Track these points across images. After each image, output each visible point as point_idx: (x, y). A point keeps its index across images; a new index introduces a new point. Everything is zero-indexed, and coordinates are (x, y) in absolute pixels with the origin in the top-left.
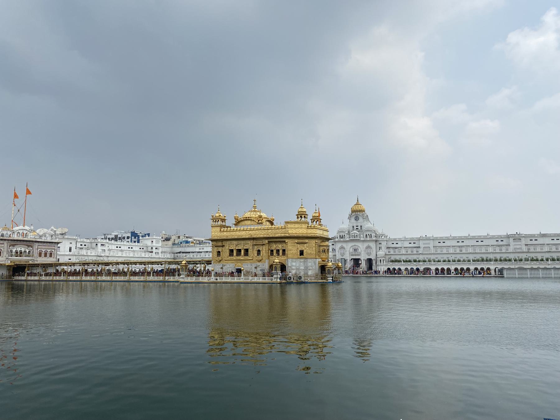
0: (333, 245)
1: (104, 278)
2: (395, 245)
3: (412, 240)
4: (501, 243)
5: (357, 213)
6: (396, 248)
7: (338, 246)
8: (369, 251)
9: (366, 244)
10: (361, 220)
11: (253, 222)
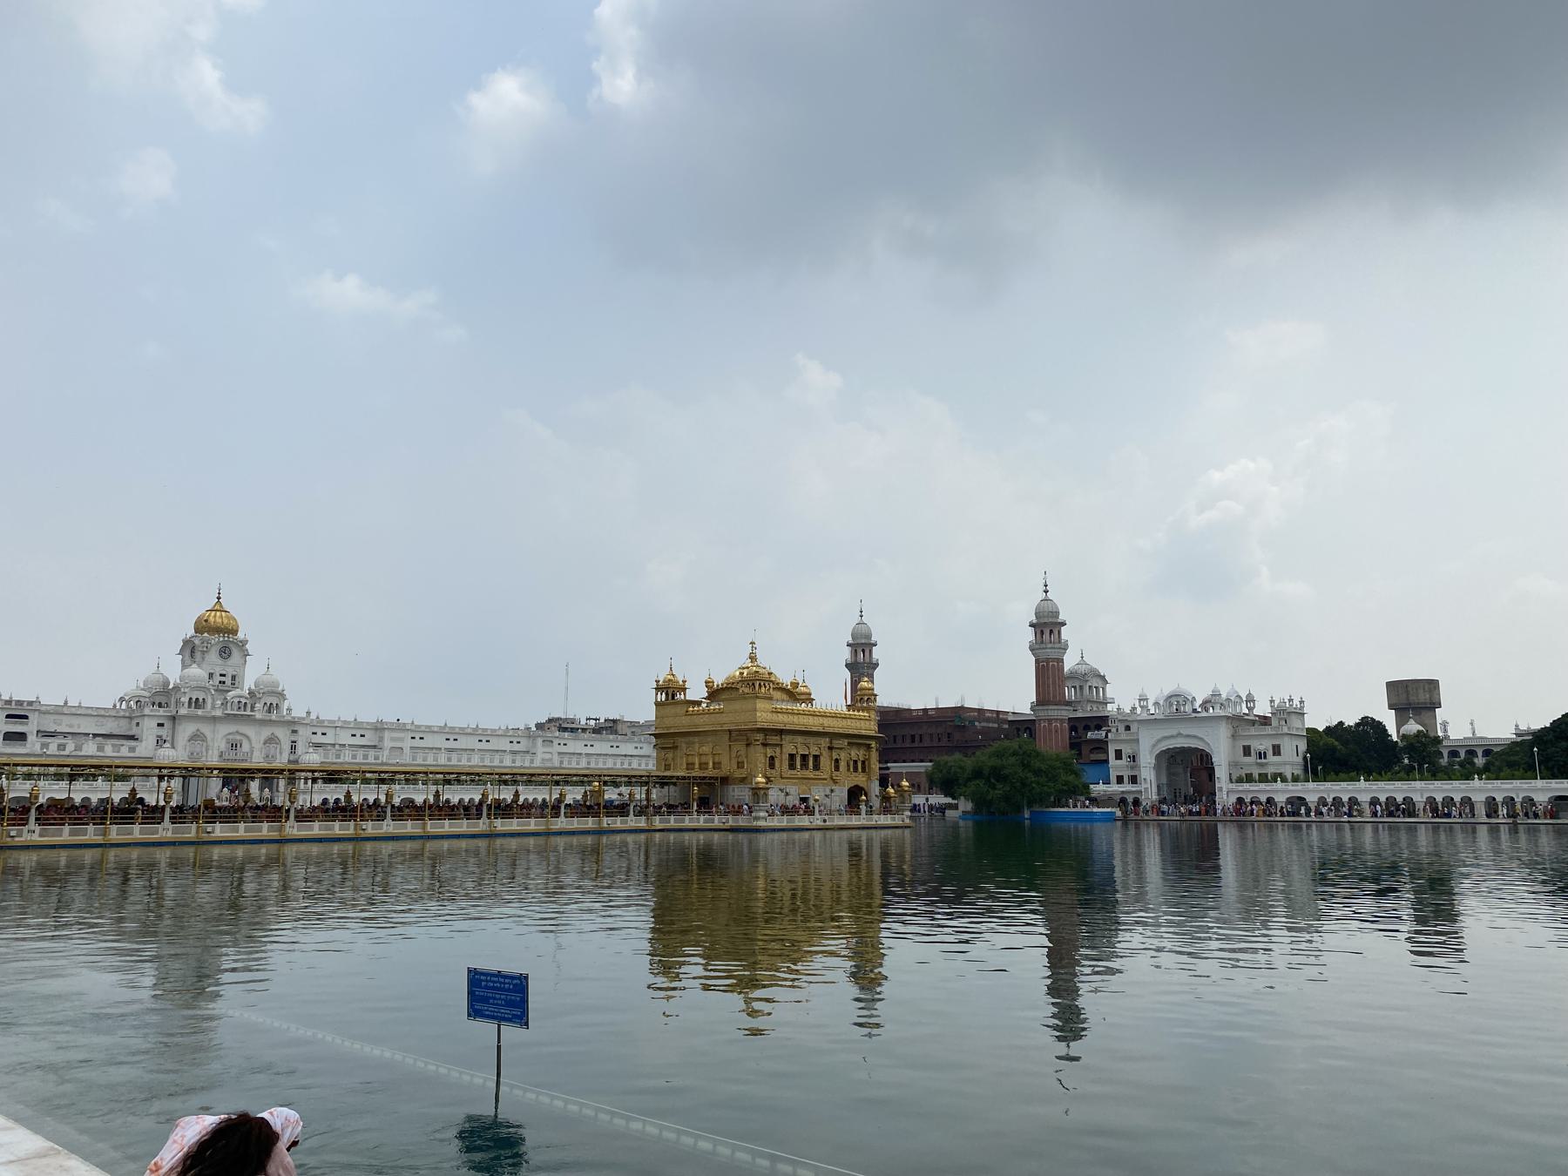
0: (161, 725)
1: (389, 826)
2: (319, 739)
3: (357, 727)
4: (516, 747)
5: (215, 636)
7: (186, 730)
8: (272, 748)
9: (266, 732)
11: (785, 697)
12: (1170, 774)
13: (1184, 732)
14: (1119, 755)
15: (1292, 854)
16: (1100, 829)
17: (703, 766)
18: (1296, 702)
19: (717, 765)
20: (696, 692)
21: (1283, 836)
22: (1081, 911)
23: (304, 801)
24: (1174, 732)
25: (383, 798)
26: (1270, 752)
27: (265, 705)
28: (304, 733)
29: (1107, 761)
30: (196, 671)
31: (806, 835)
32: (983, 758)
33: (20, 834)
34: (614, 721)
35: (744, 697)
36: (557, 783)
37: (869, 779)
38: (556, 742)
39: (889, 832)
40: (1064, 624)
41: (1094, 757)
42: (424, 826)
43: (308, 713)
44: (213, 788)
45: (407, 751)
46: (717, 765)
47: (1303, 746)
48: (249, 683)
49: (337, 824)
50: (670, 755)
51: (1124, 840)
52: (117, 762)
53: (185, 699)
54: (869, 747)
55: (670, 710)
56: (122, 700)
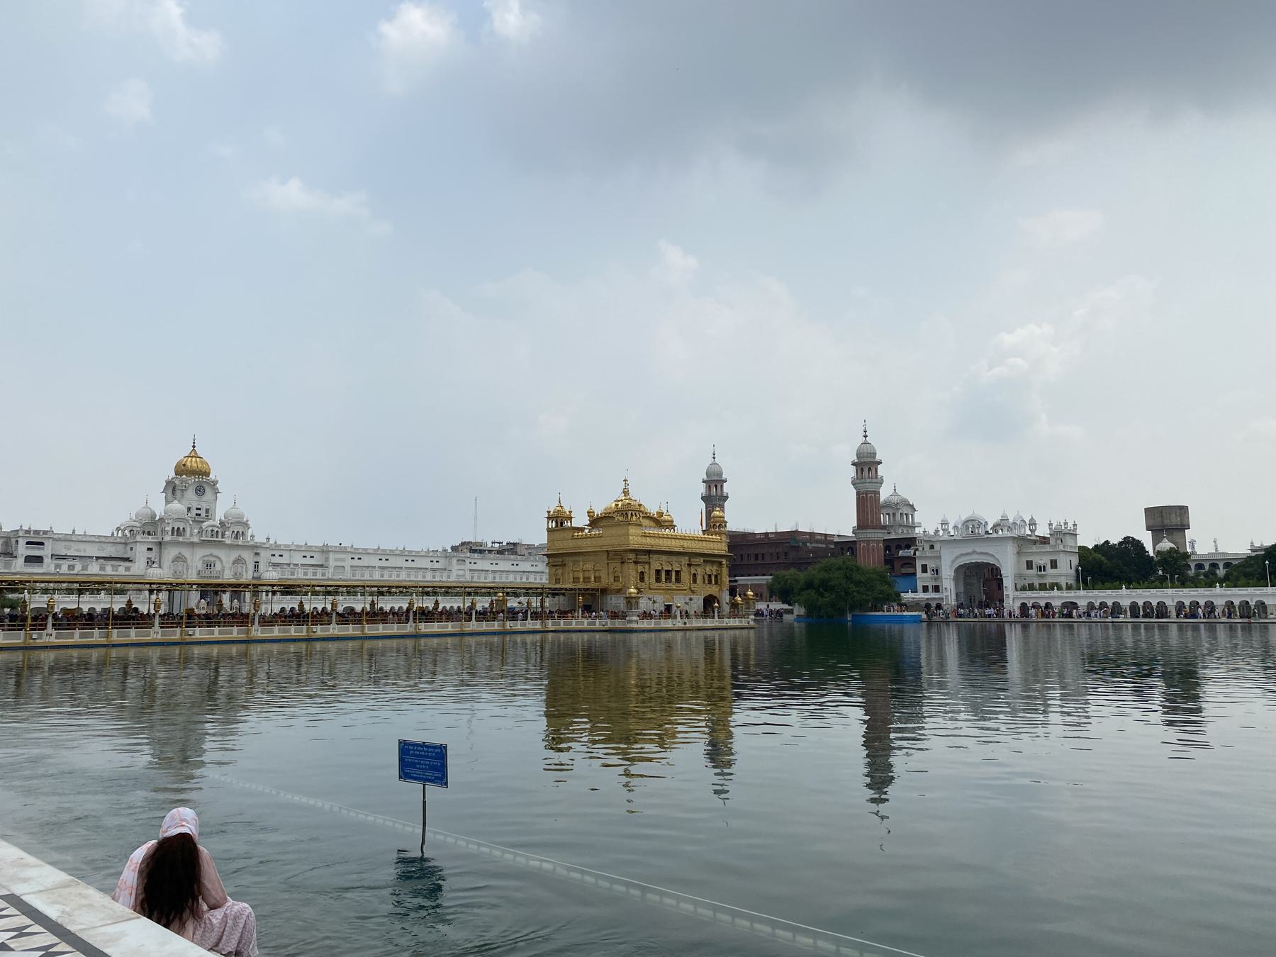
1: (334, 629)
2: (277, 560)
3: (307, 550)
4: (436, 566)
5: (192, 477)
6: (275, 565)
7: (170, 553)
9: (234, 555)
10: (209, 494)
11: (652, 524)
12: (966, 584)
13: (978, 550)
14: (924, 569)
15: (1066, 648)
16: (909, 630)
17: (586, 580)
18: (1070, 525)
19: (597, 579)
20: (581, 520)
21: (1058, 632)
22: (893, 692)
23: (265, 609)
24: (970, 550)
25: (329, 607)
26: (1049, 566)
27: (233, 533)
28: (265, 556)
29: (915, 574)
30: (178, 506)
31: (669, 634)
32: (813, 572)
33: (40, 637)
34: (515, 544)
35: (619, 524)
36: (469, 594)
37: (721, 590)
38: (468, 561)
39: (737, 632)
40: (880, 463)
41: (904, 570)
42: (363, 630)
43: (268, 539)
44: (194, 601)
45: (348, 569)
46: (597, 579)
47: (1075, 561)
48: (219, 515)
49: (293, 628)
50: (560, 571)
51: (929, 638)
52: (116, 579)
53: (169, 529)
54: (720, 564)
55: (559, 535)
56: (118, 529)
